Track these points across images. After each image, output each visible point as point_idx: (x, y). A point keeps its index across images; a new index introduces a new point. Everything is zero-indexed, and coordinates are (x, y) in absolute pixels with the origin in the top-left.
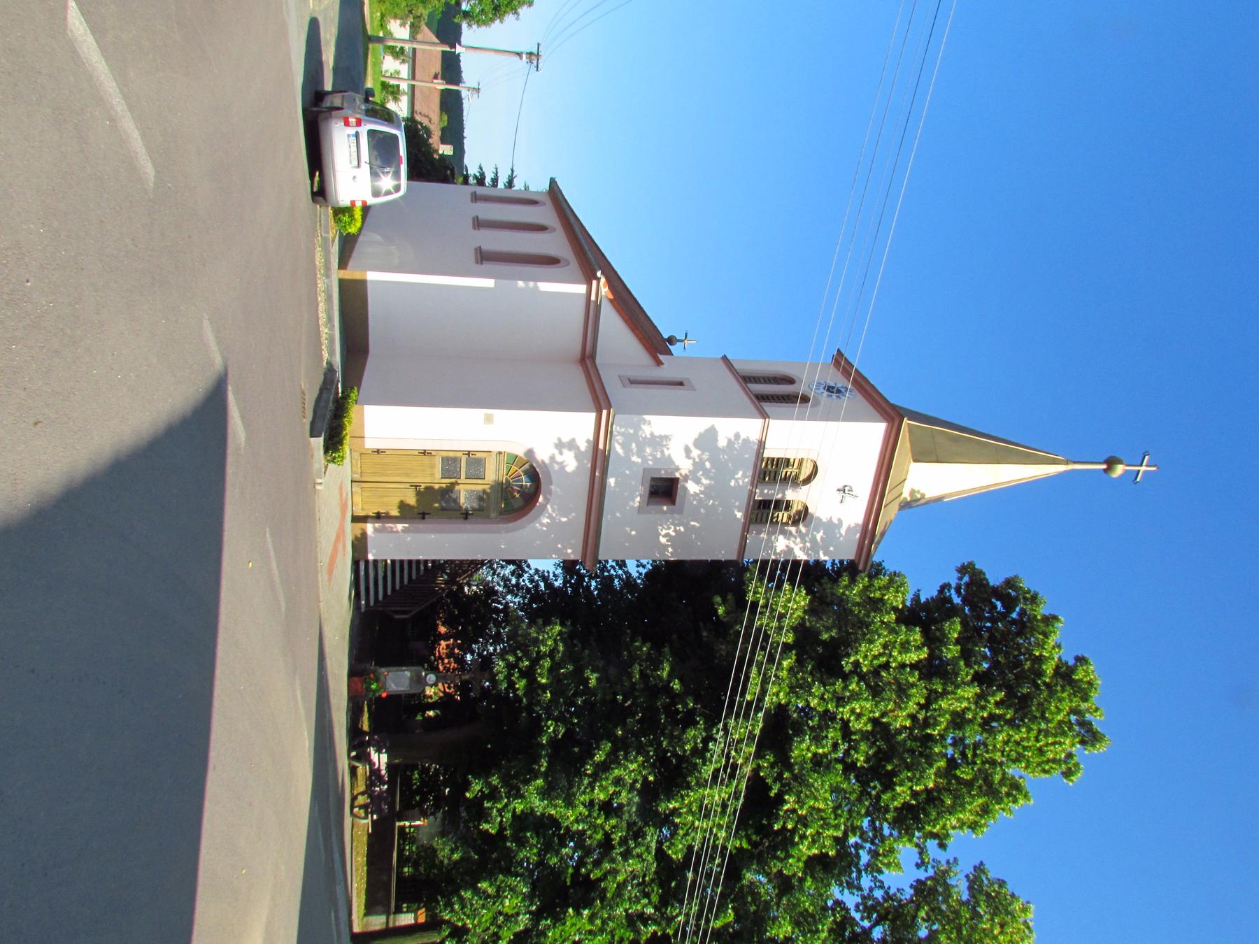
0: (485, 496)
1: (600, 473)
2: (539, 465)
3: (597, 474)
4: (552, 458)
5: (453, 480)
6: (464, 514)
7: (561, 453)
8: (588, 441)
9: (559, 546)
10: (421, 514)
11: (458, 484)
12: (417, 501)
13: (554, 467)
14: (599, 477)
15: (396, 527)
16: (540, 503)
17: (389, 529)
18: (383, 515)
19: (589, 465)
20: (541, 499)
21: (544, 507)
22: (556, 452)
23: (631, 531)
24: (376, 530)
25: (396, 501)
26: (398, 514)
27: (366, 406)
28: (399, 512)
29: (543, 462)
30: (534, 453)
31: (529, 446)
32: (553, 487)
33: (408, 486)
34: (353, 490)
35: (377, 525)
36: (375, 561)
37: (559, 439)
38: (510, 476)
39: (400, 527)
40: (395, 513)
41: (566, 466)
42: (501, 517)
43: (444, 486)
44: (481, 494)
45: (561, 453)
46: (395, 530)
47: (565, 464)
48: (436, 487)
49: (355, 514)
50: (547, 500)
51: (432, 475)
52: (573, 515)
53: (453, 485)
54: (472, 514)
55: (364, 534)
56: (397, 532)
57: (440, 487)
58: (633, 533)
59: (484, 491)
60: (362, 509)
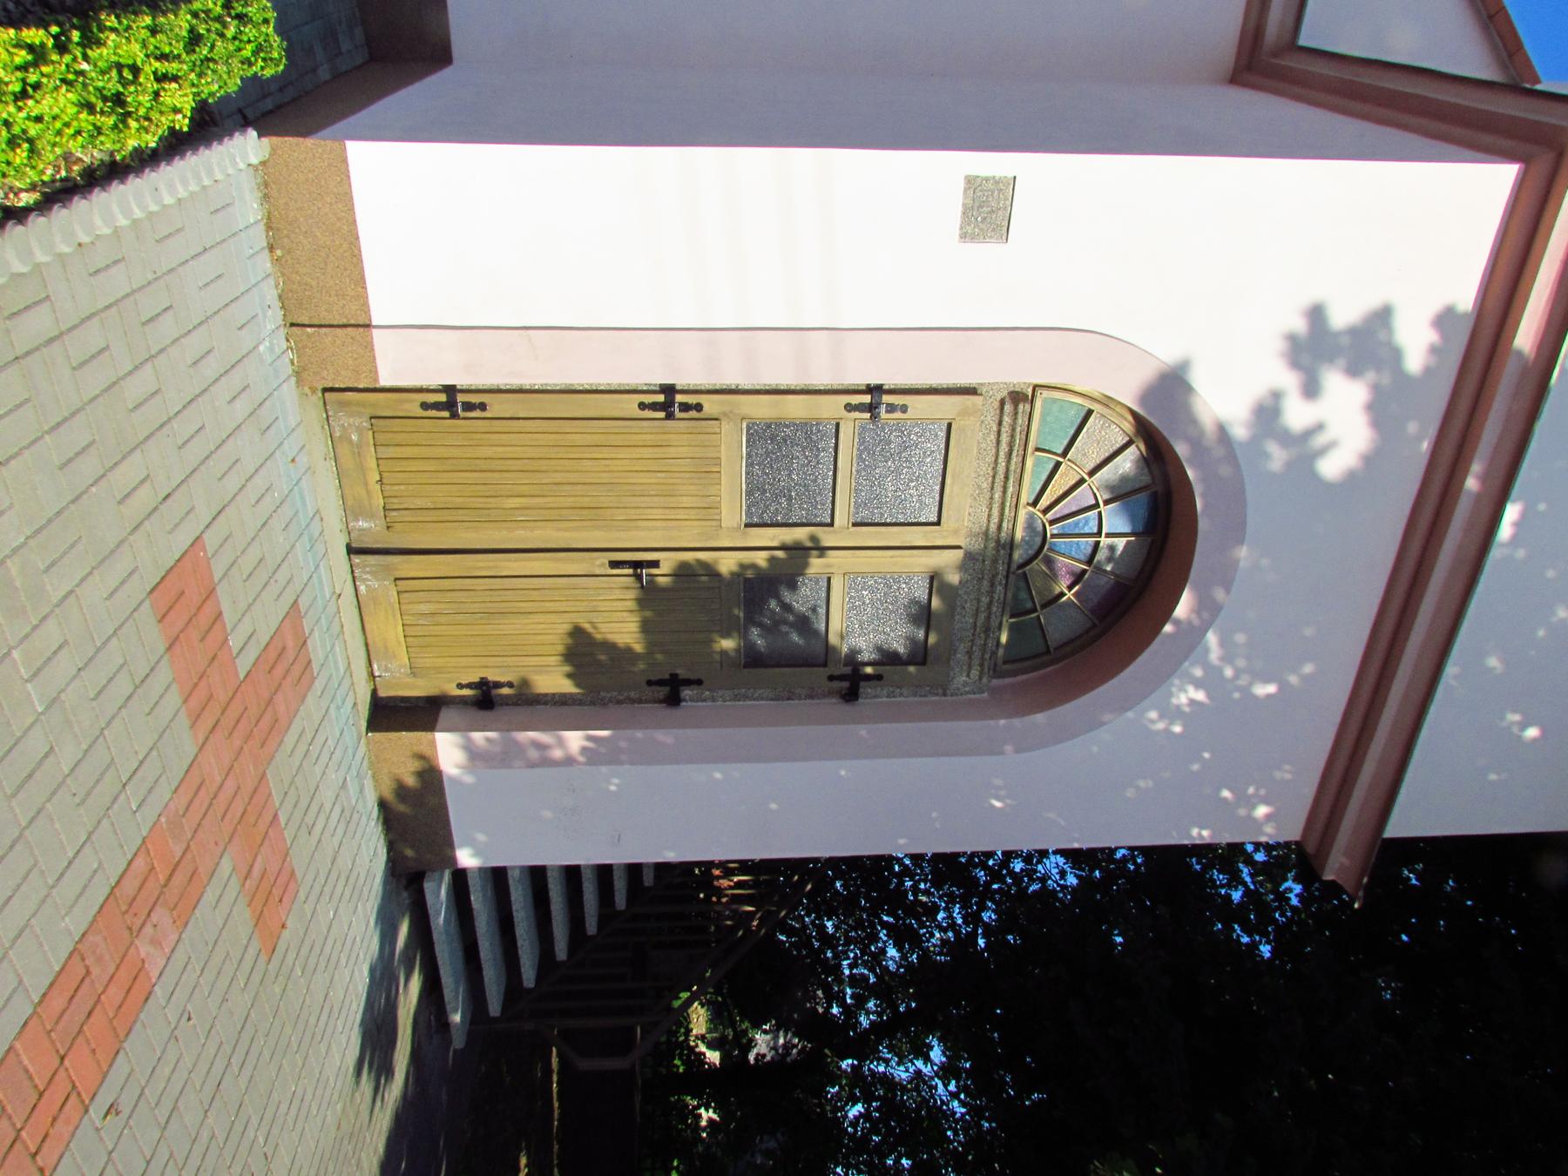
0: (936, 603)
1: (1484, 479)
2: (1196, 443)
3: (1471, 483)
4: (1267, 413)
5: (800, 534)
6: (841, 678)
7: (1311, 390)
8: (1446, 319)
9: (1226, 794)
10: (660, 683)
11: (822, 550)
12: (646, 627)
13: (1266, 456)
14: (1478, 497)
15: (561, 743)
16: (1177, 623)
17: (533, 754)
18: (505, 691)
19: (1425, 446)
20: (1183, 609)
21: (1192, 636)
22: (1288, 381)
23: (1524, 726)
24: (475, 756)
25: (553, 632)
26: (567, 687)
27: (358, 151)
28: (569, 676)
29: (1222, 431)
30: (1188, 389)
31: (1168, 355)
32: (1243, 553)
33: (600, 562)
34: (362, 589)
35: (478, 736)
36: (498, 876)
37: (1316, 314)
38: (1045, 511)
39: (575, 740)
40: (554, 680)
41: (1323, 451)
42: (995, 682)
43: (760, 559)
44: (921, 594)
45: (1311, 390)
46: (557, 754)
47: (1320, 440)
48: (727, 564)
49: (382, 693)
50: (1209, 610)
51: (710, 511)
52: (1308, 668)
53: (799, 553)
54: (878, 677)
55: (431, 776)
56: (569, 761)
57: (743, 567)
58: (1532, 732)
59: (934, 578)
60: (414, 671)
